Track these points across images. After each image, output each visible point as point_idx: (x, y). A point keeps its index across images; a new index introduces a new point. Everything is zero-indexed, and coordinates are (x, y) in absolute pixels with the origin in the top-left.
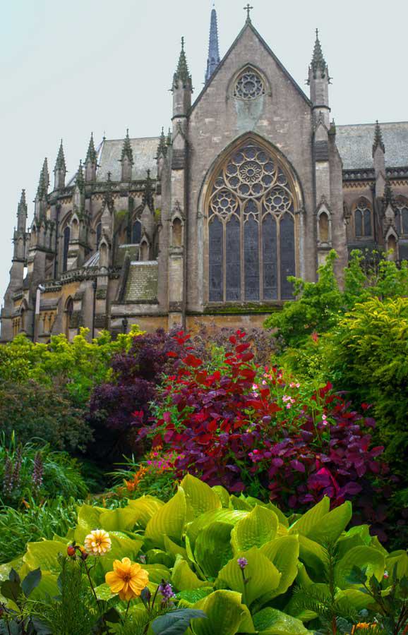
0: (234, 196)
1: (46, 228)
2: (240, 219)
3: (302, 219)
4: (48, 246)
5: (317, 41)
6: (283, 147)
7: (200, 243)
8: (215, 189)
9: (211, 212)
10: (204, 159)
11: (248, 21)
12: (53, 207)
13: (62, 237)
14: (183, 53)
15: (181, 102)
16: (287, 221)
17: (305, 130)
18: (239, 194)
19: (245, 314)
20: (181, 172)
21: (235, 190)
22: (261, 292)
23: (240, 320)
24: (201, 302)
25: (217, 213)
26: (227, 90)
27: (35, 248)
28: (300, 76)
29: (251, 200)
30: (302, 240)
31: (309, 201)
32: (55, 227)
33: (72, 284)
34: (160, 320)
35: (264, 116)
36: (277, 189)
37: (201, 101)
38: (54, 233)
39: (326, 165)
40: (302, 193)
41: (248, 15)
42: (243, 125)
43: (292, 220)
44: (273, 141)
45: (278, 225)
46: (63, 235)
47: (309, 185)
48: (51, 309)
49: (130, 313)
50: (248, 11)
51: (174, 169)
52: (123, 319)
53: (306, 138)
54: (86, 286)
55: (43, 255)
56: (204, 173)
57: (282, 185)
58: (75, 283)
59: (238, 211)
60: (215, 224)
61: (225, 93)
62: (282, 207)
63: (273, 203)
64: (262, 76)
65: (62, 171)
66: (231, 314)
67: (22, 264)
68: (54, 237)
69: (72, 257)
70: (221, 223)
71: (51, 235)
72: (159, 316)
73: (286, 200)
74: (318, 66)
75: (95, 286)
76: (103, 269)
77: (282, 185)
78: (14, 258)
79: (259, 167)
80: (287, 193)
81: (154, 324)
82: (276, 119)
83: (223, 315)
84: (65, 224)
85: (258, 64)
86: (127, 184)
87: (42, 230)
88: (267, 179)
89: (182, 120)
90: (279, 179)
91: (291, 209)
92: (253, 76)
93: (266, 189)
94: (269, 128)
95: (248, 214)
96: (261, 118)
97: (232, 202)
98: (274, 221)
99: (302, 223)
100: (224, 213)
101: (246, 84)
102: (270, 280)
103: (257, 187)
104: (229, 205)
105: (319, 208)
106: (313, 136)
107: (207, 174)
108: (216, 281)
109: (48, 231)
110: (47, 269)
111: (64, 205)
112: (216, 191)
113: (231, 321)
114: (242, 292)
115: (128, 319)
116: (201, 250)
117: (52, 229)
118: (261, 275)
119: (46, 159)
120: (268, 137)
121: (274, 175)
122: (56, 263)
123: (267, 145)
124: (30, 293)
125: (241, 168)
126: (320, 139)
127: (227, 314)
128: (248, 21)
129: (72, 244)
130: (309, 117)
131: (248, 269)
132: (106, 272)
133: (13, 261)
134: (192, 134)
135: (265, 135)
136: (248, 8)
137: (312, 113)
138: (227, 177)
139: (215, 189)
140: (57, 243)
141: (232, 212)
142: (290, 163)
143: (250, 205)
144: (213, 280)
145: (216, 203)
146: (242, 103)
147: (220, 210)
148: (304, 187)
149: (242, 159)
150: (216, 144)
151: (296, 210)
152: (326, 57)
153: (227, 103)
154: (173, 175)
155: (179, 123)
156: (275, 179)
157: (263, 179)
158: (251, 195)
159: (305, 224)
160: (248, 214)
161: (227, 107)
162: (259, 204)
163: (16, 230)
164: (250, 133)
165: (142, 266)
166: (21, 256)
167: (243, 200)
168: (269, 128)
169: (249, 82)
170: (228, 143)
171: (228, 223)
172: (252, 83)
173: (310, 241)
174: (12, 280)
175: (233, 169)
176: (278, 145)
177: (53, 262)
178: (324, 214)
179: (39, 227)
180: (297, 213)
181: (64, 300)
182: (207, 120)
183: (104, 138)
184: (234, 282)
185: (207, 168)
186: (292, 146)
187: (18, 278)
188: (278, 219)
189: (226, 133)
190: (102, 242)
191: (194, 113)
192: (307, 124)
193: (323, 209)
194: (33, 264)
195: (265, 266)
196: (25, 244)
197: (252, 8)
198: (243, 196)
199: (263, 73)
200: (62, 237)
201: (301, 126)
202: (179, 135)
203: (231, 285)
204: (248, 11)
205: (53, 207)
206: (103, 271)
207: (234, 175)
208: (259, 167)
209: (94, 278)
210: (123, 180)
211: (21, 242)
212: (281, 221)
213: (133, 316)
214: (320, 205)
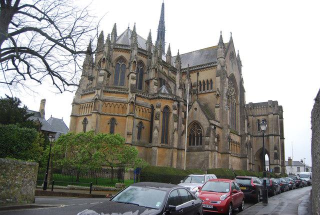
14: (221, 36)
54: (176, 104)
119: (115, 24)
181: (163, 106)
183: (129, 27)
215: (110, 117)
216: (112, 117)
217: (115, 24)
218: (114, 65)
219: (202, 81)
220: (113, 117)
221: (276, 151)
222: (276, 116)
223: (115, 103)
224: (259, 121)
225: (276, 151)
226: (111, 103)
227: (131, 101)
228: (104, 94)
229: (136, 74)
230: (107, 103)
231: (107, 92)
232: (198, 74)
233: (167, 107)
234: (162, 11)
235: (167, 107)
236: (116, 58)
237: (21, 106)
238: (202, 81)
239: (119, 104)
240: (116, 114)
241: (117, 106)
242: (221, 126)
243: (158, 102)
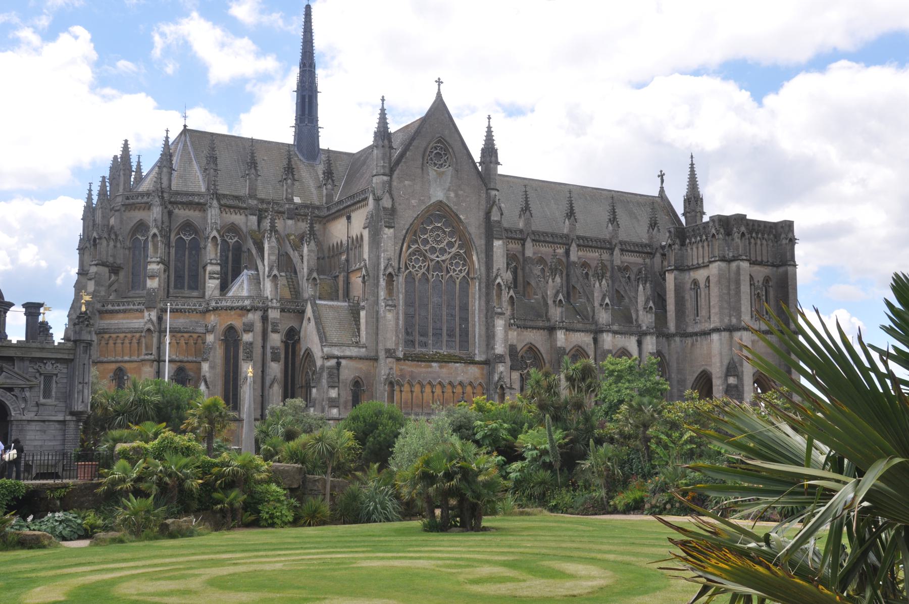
0: (425, 256)
2: (430, 277)
3: (477, 284)
5: (489, 128)
6: (465, 219)
7: (401, 296)
8: (411, 247)
9: (407, 268)
10: (406, 217)
11: (439, 95)
15: (387, 161)
16: (466, 282)
17: (482, 207)
18: (428, 255)
19: (436, 362)
20: (392, 230)
21: (426, 251)
22: (445, 343)
23: (431, 367)
24: (401, 349)
25: (411, 269)
26: (423, 158)
27: (158, 260)
28: (477, 157)
29: (438, 262)
30: (477, 302)
31: (483, 269)
33: (233, 312)
34: (367, 363)
35: (452, 188)
36: (457, 255)
37: (402, 164)
39: (500, 242)
40: (479, 262)
41: (439, 89)
42: (438, 194)
43: (468, 283)
44: (458, 213)
45: (458, 286)
47: (483, 256)
48: (180, 332)
49: (342, 354)
50: (439, 85)
51: (386, 227)
52: (335, 360)
53: (482, 214)
56: (404, 232)
57: (461, 251)
58: (238, 311)
59: (428, 270)
60: (410, 279)
61: (421, 160)
62: (461, 271)
63: (458, 269)
64: (450, 150)
66: (424, 361)
69: (214, 278)
70: (414, 279)
72: (367, 359)
73: (464, 265)
74: (490, 151)
75: (265, 319)
76: (275, 301)
77: (461, 251)
79: (444, 232)
80: (465, 259)
81: (363, 366)
82: (460, 192)
83: (418, 361)
85: (447, 139)
86: (255, 202)
88: (451, 245)
89: (385, 178)
90: (460, 247)
91: (468, 273)
92: (442, 148)
93: (450, 253)
94: (455, 200)
95: (435, 274)
96: (449, 190)
97: (424, 261)
98: (454, 282)
99: (477, 288)
100: (417, 271)
101: (436, 154)
102: (451, 334)
103: (443, 251)
104: (420, 264)
105: (496, 278)
106: (488, 214)
107: (407, 233)
108: (409, 330)
112: (411, 250)
113: (424, 367)
114: (430, 342)
115: (341, 360)
116: (401, 302)
118: (445, 329)
119: (126, 141)
120: (454, 208)
121: (455, 241)
122: (168, 276)
123: (453, 215)
125: (432, 230)
126: (495, 219)
127: (421, 361)
128: (439, 95)
129: (211, 263)
130: (484, 196)
131: (435, 322)
132: (278, 305)
134: (395, 193)
135: (451, 205)
136: (439, 82)
137: (487, 193)
138: (420, 237)
139: (411, 247)
140: (169, 253)
141: (423, 270)
142: (470, 234)
143: (438, 266)
144: (406, 329)
145: (411, 260)
146: (435, 173)
147: (414, 267)
148: (480, 256)
149: (431, 223)
150: (414, 206)
151: (472, 275)
152: (498, 144)
153: (423, 170)
154: (385, 232)
155: (384, 183)
156: (457, 245)
157: (447, 244)
158: (438, 257)
159: (480, 289)
160: (435, 274)
161: (423, 173)
162: (444, 266)
164: (441, 201)
165: (327, 305)
167: (432, 260)
168: (455, 200)
169: (438, 153)
170: (423, 207)
171: (420, 280)
172: (441, 154)
173: (483, 303)
174: (97, 288)
175: (425, 231)
176: (461, 216)
178: (499, 283)
180: (472, 279)
181: (221, 328)
182: (406, 182)
183: (185, 126)
184: (424, 334)
185: (407, 227)
186: (472, 221)
188: (458, 281)
189: (422, 198)
190: (273, 274)
191: (396, 173)
192: (483, 202)
193: (499, 280)
194: (157, 279)
195: (447, 321)
197: (442, 83)
198: (443, 258)
199: (452, 148)
201: (479, 203)
202: (387, 194)
203: (421, 335)
204: (439, 85)
206: (275, 304)
207: (425, 237)
208: (444, 232)
209: (265, 310)
210: (252, 196)
212: (460, 283)
213: (344, 358)
214: (497, 276)
215: (114, 366)
216: (118, 365)
217: (126, 141)
218: (128, 243)
219: (354, 238)
220: (118, 365)
221: (732, 380)
222: (734, 265)
223: (122, 335)
224: (695, 282)
225: (732, 380)
226: (114, 336)
227: (146, 328)
228: (101, 319)
229: (158, 263)
230: (107, 336)
231: (107, 312)
232: (349, 218)
233: (231, 329)
234: (305, 32)
235: (231, 329)
236: (129, 227)
237: (51, 331)
238: (354, 238)
239: (129, 335)
240: (126, 358)
241: (127, 341)
242: (373, 354)
243: (212, 319)
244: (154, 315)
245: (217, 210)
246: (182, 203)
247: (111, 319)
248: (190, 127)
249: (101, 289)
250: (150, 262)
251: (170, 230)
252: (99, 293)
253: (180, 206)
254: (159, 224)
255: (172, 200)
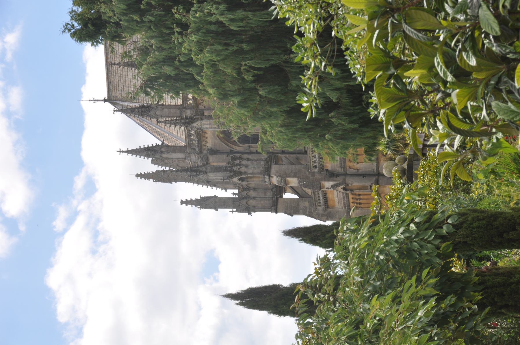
1: (239, 165)
4: (263, 163)
12: (211, 158)
13: (249, 147)
27: (266, 177)
32: (238, 155)
38: (245, 156)
46: (247, 145)
55: (274, 168)
65: (163, 150)
67: (280, 200)
68: (250, 157)
71: (248, 159)
78: (272, 211)
84: (234, 143)
87: (243, 169)
109: (244, 162)
110: (291, 163)
111: (209, 145)
117: (240, 158)
119: (137, 176)
124: (325, 181)
133: (276, 213)
163: (235, 210)
166: (269, 202)
177: (282, 156)
179: (241, 173)
183: (105, 100)
187: (298, 205)
196: (254, 198)
200: (249, 147)
205: (211, 158)
211: (252, 202)
217: (137, 176)
228: (334, 207)
244: (327, 184)
245: (204, 122)
246: (199, 142)
247: (333, 201)
248: (105, 95)
249: (301, 207)
250: (270, 184)
251: (231, 152)
252: (306, 208)
253: (204, 143)
254: (228, 174)
255: (197, 150)
